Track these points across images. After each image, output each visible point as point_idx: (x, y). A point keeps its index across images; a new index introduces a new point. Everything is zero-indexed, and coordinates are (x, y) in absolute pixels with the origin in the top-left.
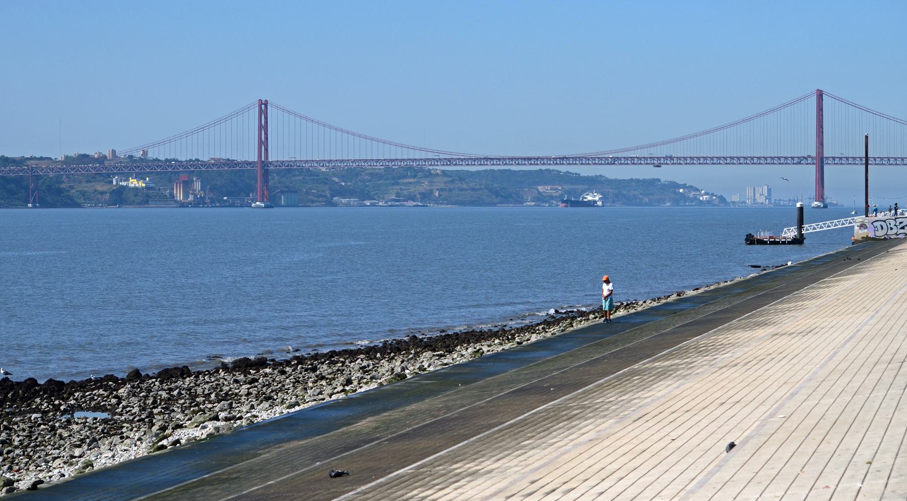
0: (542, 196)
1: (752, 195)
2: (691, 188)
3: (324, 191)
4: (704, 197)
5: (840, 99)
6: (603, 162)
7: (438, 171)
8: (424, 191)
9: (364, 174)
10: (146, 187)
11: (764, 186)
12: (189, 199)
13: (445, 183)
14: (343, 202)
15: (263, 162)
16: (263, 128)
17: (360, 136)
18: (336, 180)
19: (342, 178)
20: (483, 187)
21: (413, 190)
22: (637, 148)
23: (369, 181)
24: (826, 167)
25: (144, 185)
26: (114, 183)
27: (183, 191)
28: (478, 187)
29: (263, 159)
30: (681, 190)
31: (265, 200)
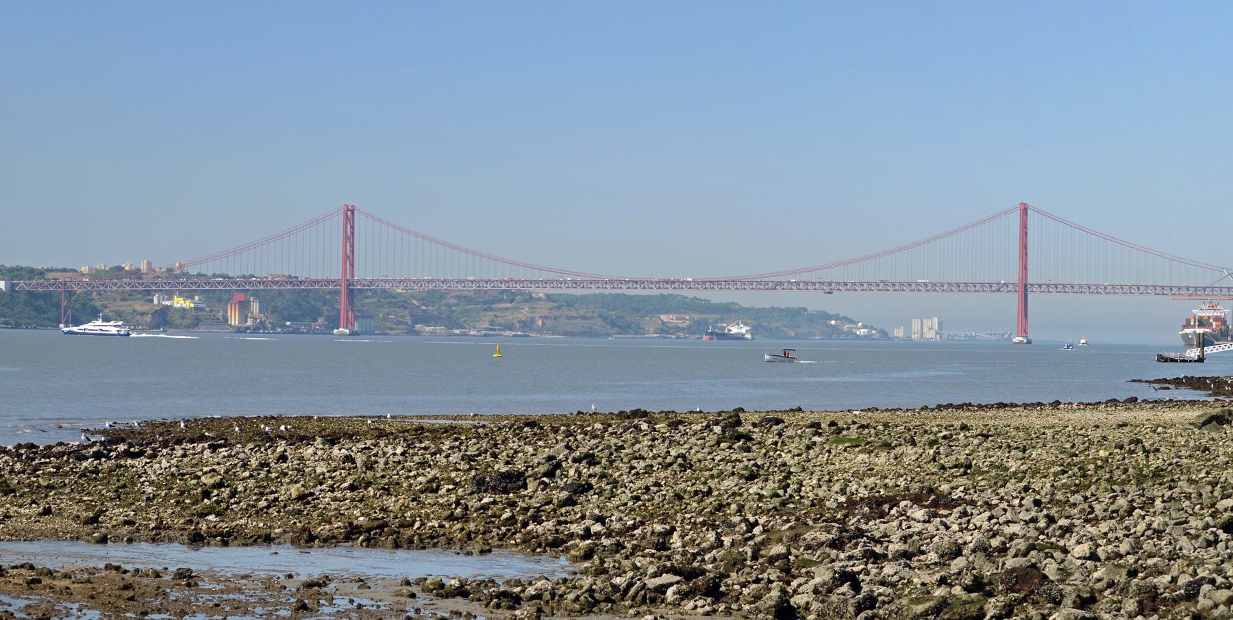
0: (667, 327)
2: (846, 319)
3: (403, 317)
4: (862, 330)
7: (541, 295)
8: (524, 319)
9: (448, 296)
10: (197, 309)
13: (550, 309)
16: (349, 238)
18: (415, 302)
20: (595, 315)
21: (510, 317)
22: (803, 271)
23: (457, 305)
24: (1030, 295)
25: (192, 305)
26: (156, 302)
28: (589, 314)
30: (833, 322)
31: (350, 326)
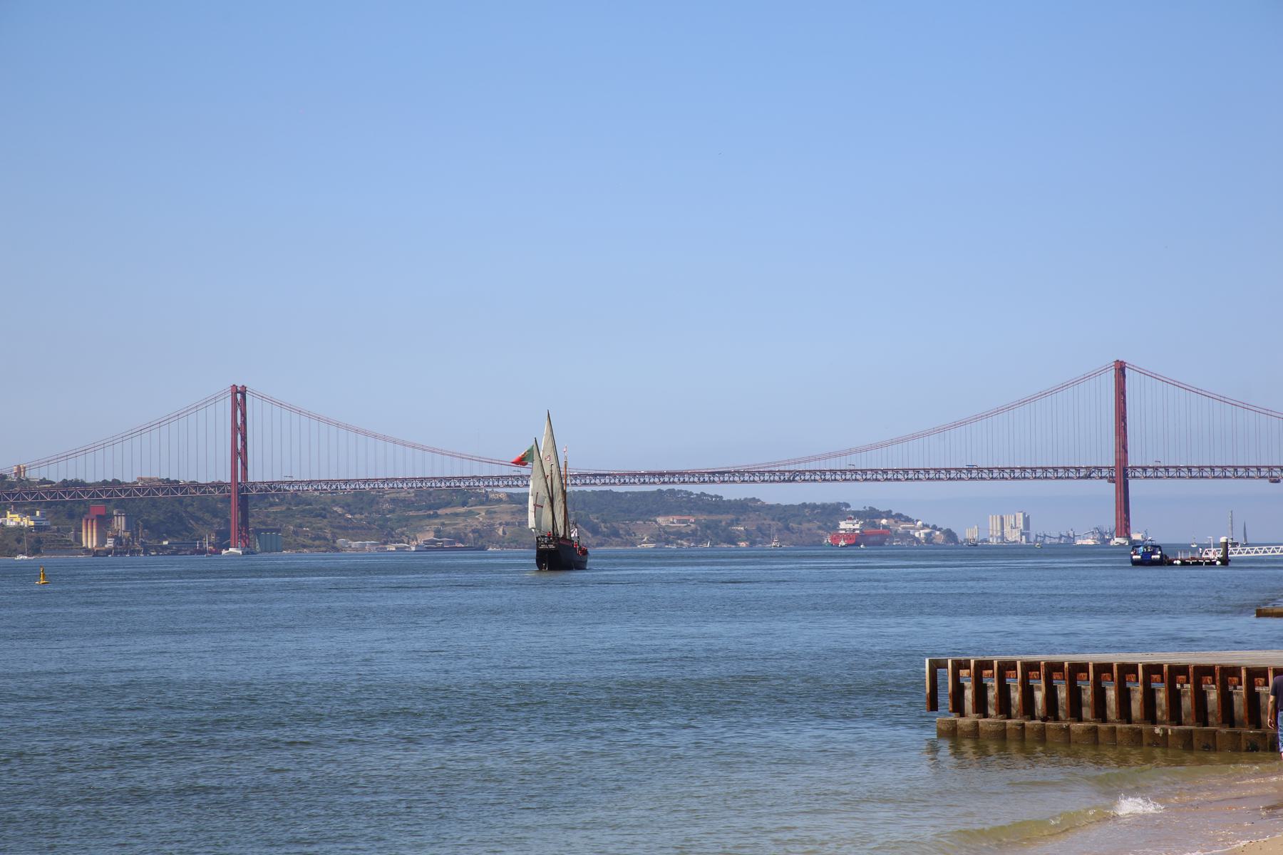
1: (999, 528)
2: (900, 517)
3: (321, 529)
4: (921, 531)
5: (1152, 375)
6: (777, 478)
8: (479, 527)
9: (381, 500)
10: (36, 527)
11: (1017, 514)
12: (106, 546)
13: (513, 513)
14: (353, 546)
15: (239, 483)
16: (240, 429)
17: (395, 442)
18: (339, 510)
19: (347, 506)
24: (1132, 484)
25: (32, 523)
27: (97, 532)
29: (239, 481)
30: (884, 522)
